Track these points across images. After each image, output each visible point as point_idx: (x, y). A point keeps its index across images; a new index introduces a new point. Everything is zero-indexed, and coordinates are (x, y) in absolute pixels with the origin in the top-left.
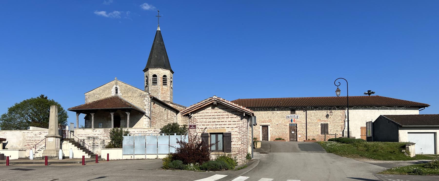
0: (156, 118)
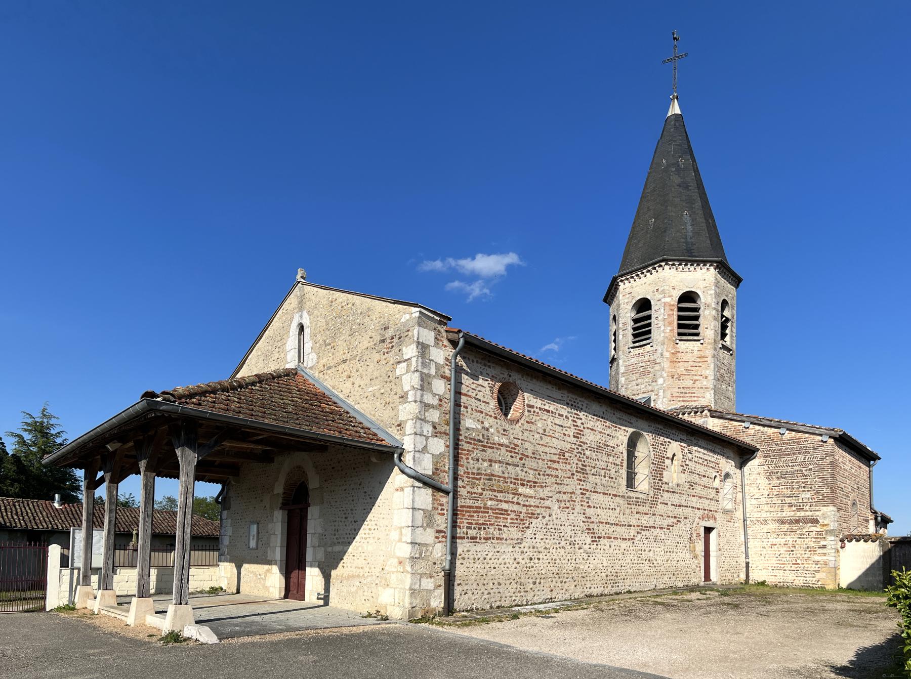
0: (533, 484)
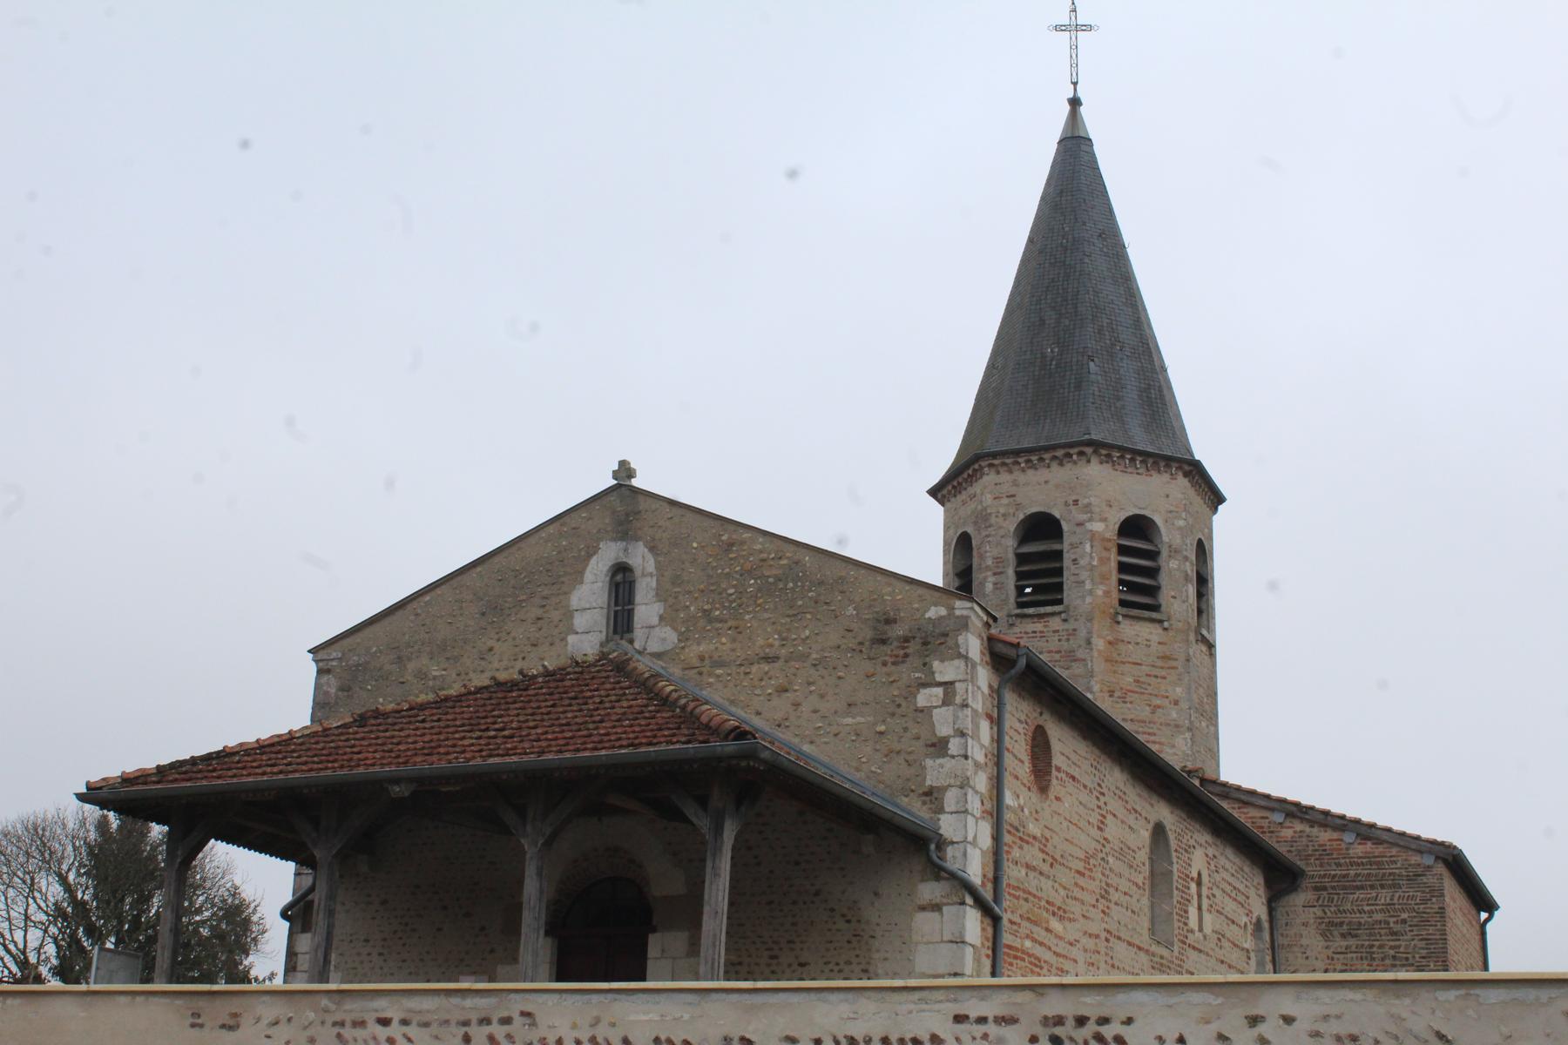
0: (1061, 914)
